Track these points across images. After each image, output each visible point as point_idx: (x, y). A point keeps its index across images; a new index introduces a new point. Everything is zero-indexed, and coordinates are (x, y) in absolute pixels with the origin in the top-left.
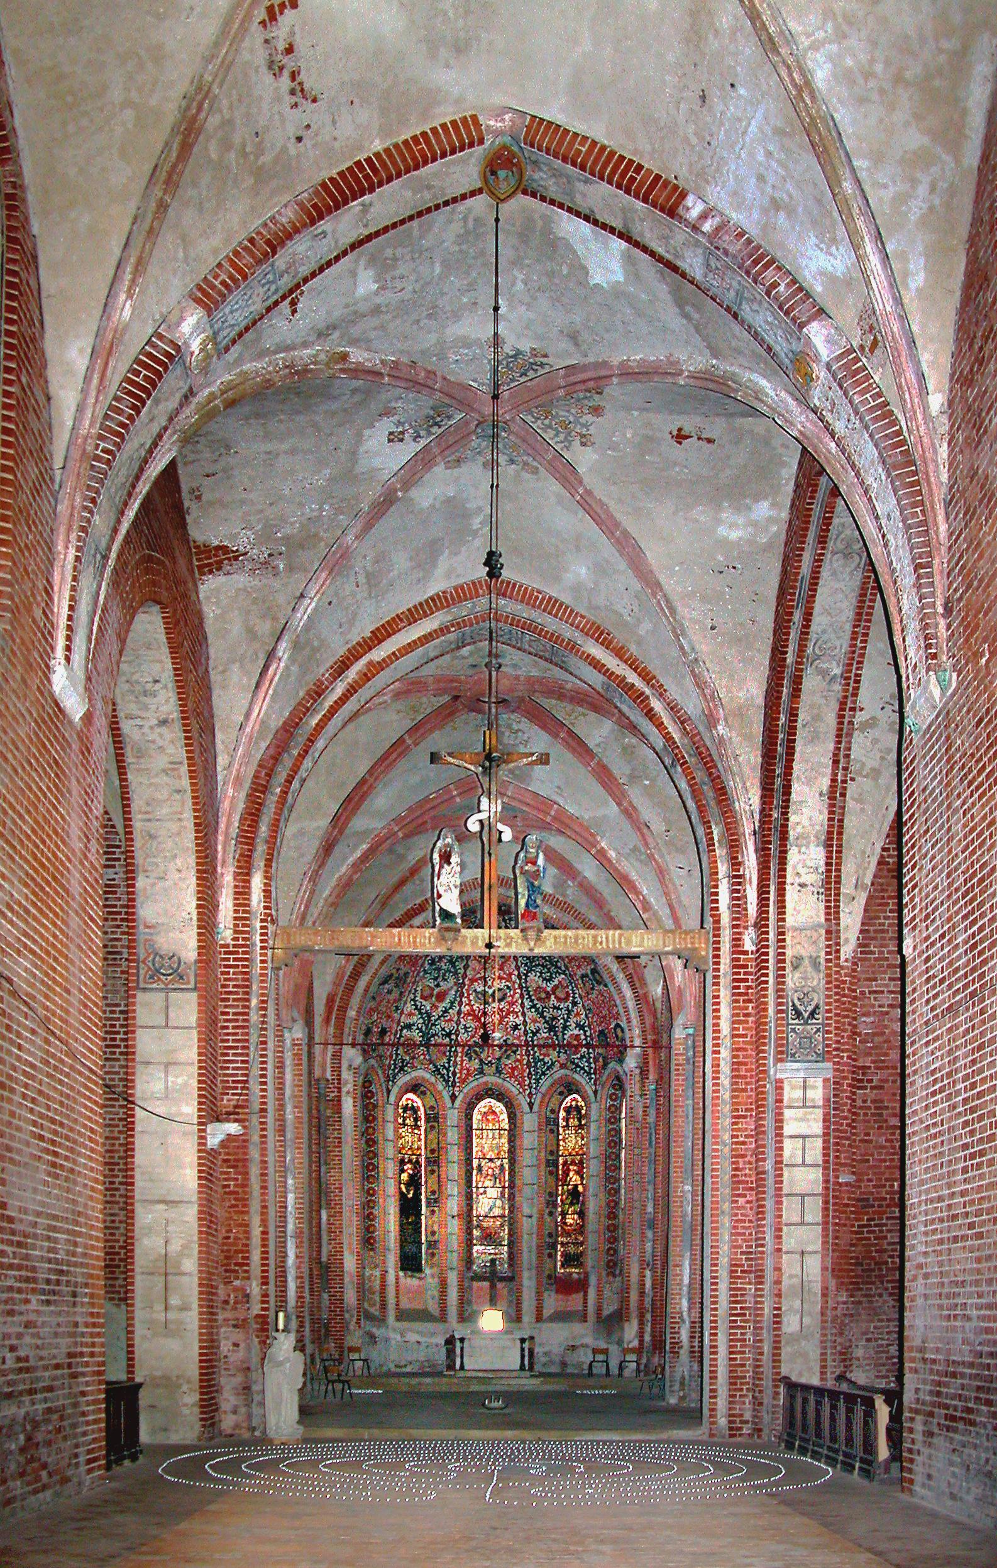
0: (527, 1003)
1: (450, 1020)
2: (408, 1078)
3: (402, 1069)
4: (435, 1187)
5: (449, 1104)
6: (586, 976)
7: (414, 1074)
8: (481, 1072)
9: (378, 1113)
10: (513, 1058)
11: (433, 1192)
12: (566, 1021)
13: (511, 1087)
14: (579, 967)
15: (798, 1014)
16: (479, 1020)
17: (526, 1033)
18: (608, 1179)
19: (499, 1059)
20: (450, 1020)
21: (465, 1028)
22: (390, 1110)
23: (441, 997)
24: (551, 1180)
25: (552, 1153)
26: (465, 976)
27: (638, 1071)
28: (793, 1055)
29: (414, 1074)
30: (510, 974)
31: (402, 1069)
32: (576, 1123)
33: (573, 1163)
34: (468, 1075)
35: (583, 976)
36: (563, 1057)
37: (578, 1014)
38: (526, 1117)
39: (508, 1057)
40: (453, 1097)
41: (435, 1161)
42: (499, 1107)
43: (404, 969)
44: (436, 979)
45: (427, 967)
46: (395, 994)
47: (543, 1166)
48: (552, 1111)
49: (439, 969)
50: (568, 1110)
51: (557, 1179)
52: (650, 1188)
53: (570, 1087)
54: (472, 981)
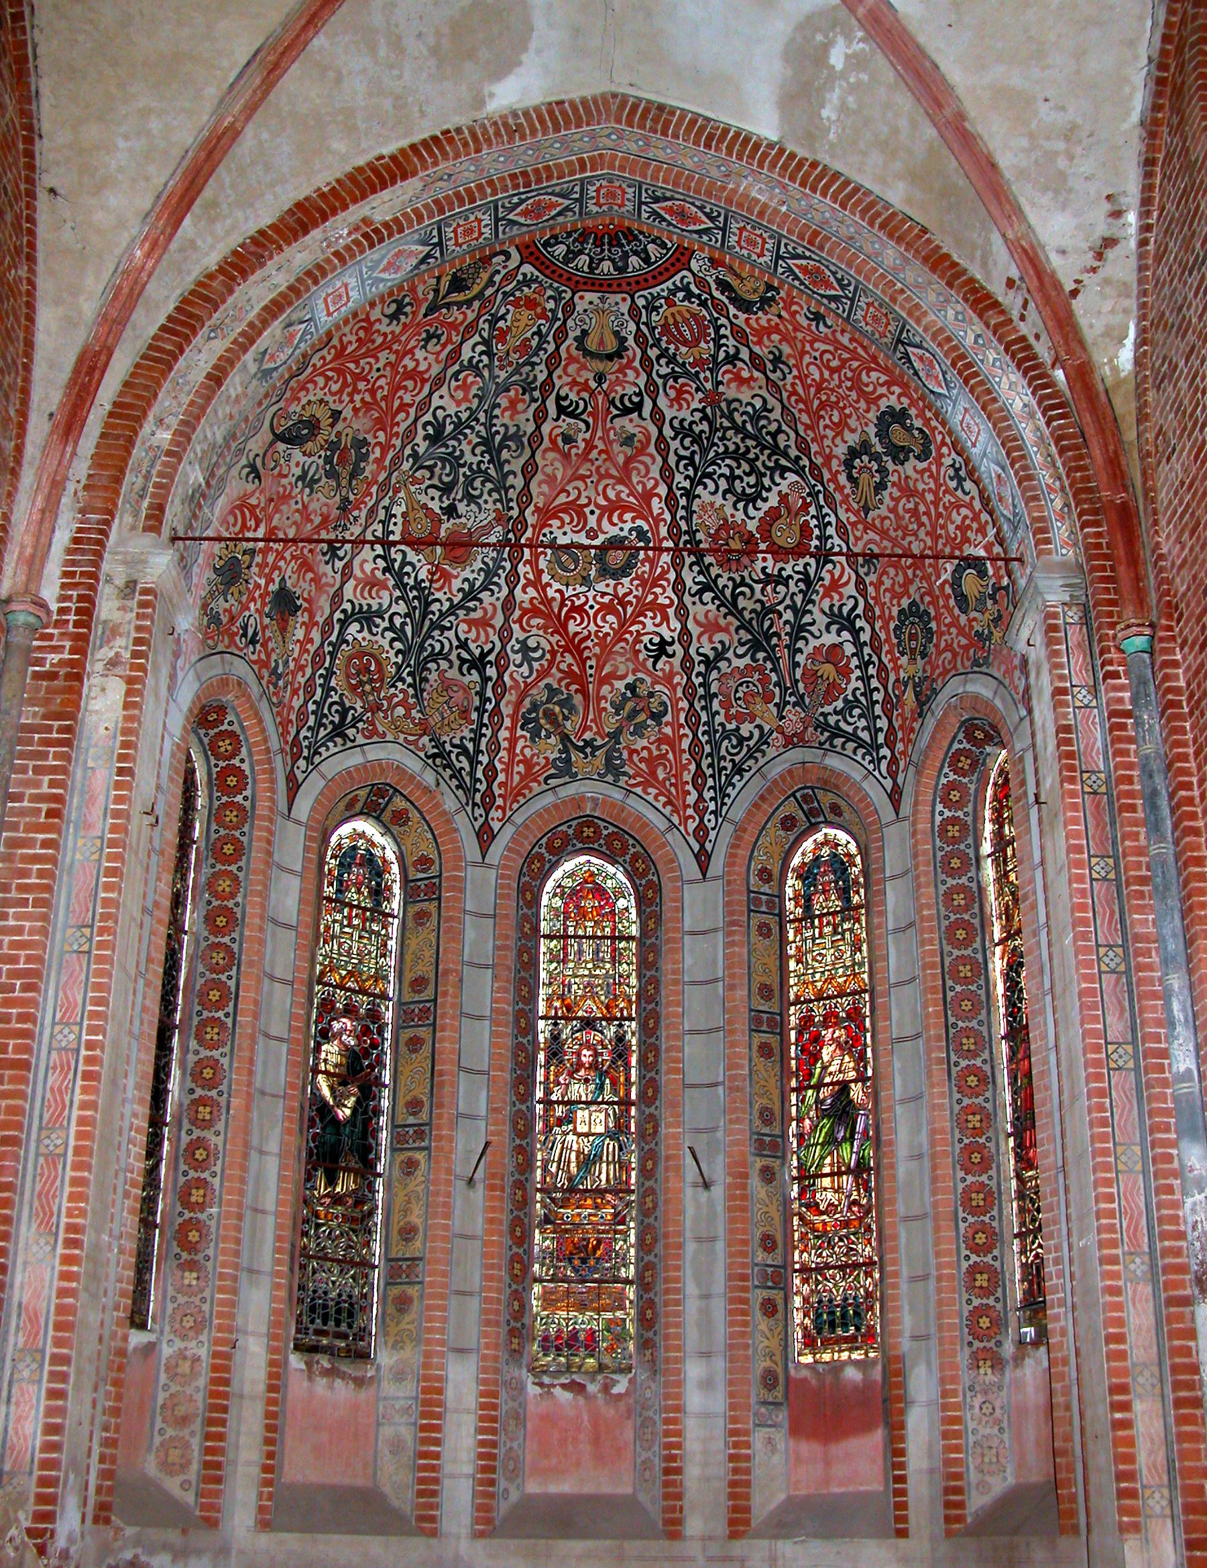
0: (690, 577)
1: (484, 623)
2: (354, 759)
3: (338, 731)
4: (421, 1092)
5: (471, 849)
6: (864, 447)
7: (375, 753)
8: (565, 769)
9: (253, 836)
10: (652, 733)
11: (414, 1105)
12: (799, 612)
13: (648, 810)
14: (840, 427)
16: (561, 627)
17: (687, 664)
18: (953, 1040)
19: (615, 736)
20: (484, 623)
21: (525, 649)
22: (292, 846)
23: (460, 547)
24: (767, 1070)
25: (766, 992)
27: (1073, 615)
29: (375, 753)
30: (648, 496)
31: (338, 731)
32: (836, 904)
33: (830, 1019)
34: (529, 775)
35: (853, 453)
36: (793, 715)
37: (835, 585)
38: (689, 893)
39: (639, 731)
40: (485, 836)
41: (422, 1013)
42: (615, 876)
43: (355, 425)
44: (446, 489)
45: (422, 447)
46: (323, 501)
47: (742, 1025)
48: (765, 875)
49: (455, 461)
50: (807, 874)
51: (785, 1073)
52: (1176, 981)
53: (813, 804)
54: (547, 514)
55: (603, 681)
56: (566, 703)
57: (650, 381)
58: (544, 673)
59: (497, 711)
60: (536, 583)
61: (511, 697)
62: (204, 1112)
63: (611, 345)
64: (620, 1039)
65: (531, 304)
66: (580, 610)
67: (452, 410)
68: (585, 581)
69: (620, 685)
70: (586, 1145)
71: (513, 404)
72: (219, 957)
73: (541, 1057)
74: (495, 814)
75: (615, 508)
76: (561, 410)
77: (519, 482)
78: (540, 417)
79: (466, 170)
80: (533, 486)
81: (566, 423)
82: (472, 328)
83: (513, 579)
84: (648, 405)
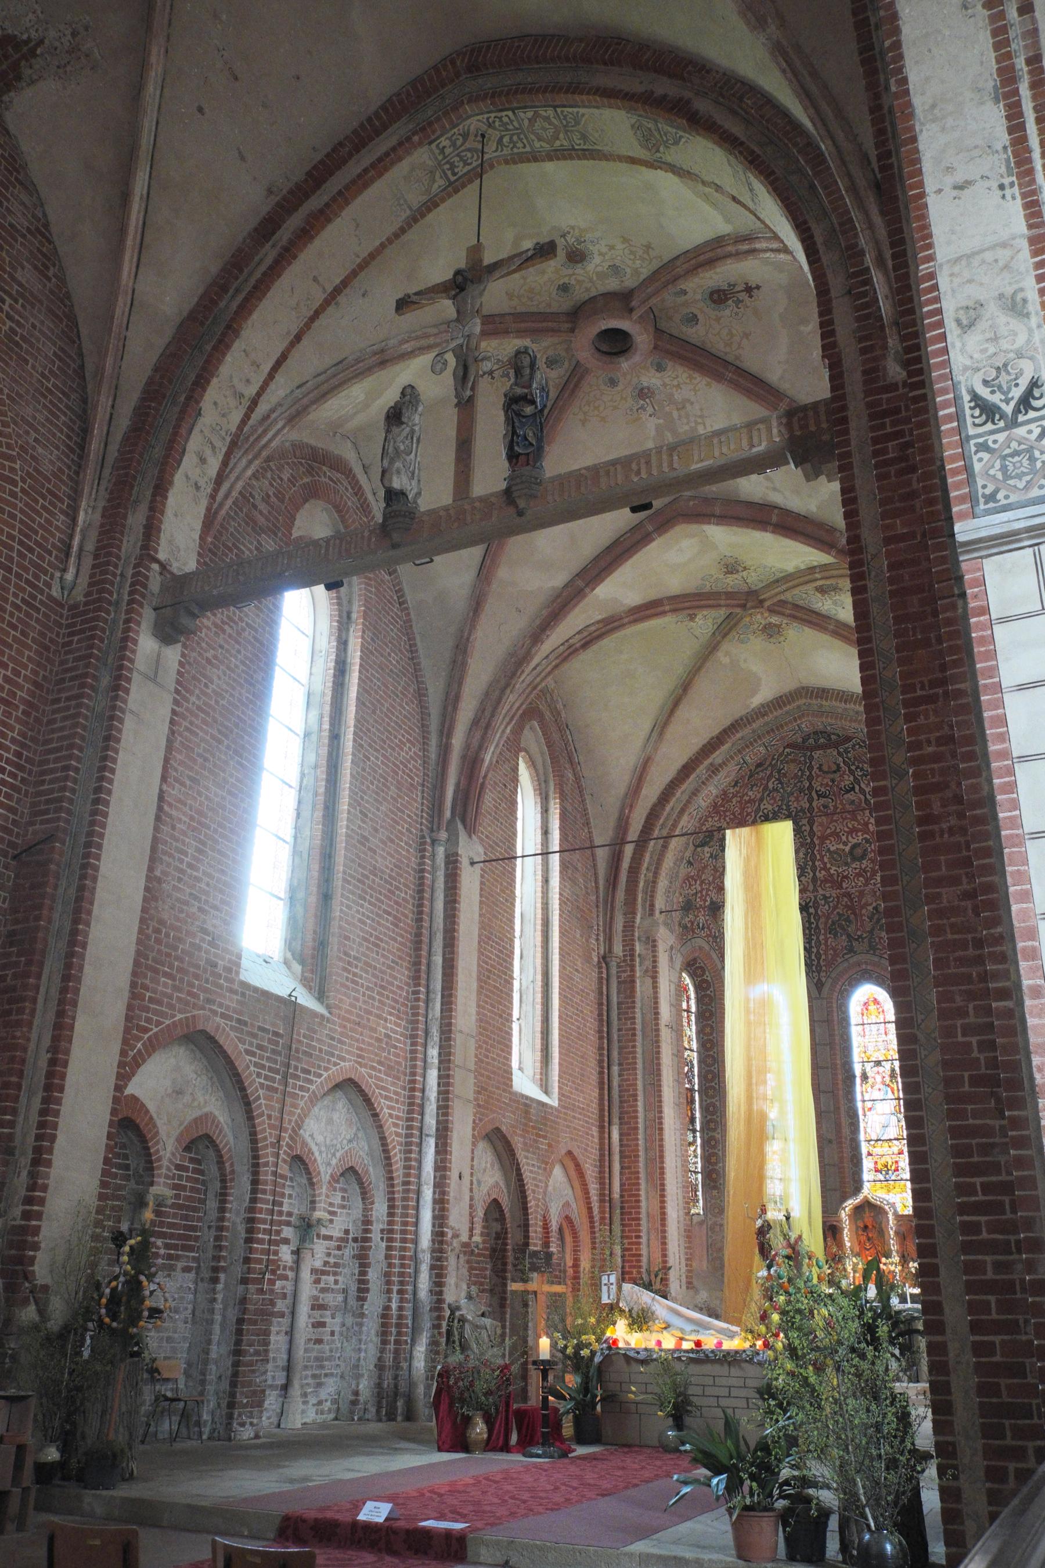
8: (851, 950)
15: (989, 411)
19: (871, 932)
21: (825, 898)
26: (812, 833)
28: (991, 497)
30: (866, 824)
54: (823, 839)
55: (862, 907)
56: (848, 920)
57: (855, 778)
58: (835, 907)
59: (817, 926)
60: (825, 868)
61: (822, 920)
62: (712, 1125)
63: (834, 768)
64: (893, 1070)
65: (792, 761)
66: (846, 877)
67: (770, 808)
68: (847, 864)
69: (870, 908)
70: (883, 1120)
71: (797, 799)
72: (709, 1061)
73: (858, 1080)
74: (823, 974)
75: (853, 831)
76: (819, 796)
77: (808, 828)
78: (810, 800)
79: (745, 732)
80: (815, 828)
81: (822, 801)
82: (771, 776)
83: (814, 869)
84: (857, 788)
